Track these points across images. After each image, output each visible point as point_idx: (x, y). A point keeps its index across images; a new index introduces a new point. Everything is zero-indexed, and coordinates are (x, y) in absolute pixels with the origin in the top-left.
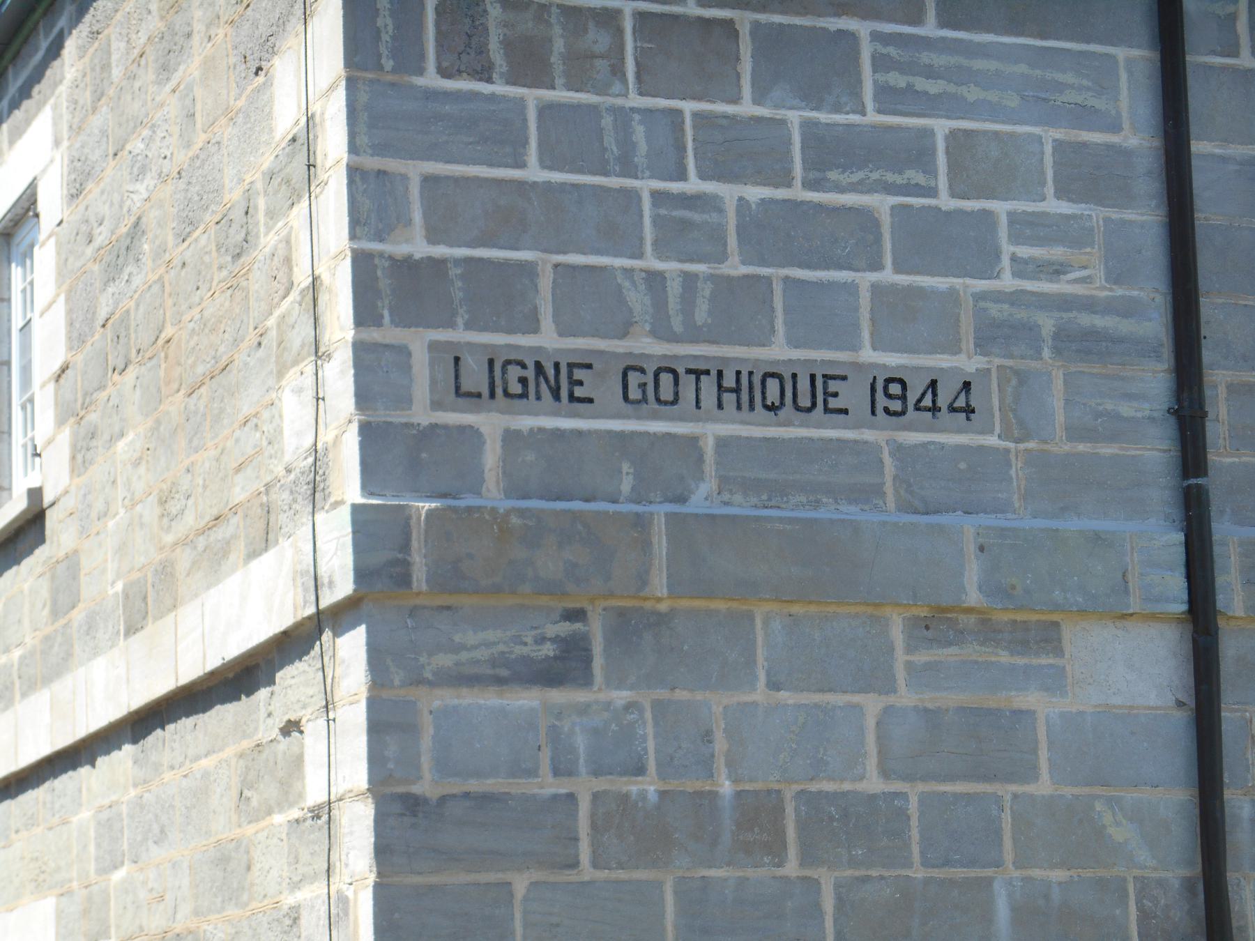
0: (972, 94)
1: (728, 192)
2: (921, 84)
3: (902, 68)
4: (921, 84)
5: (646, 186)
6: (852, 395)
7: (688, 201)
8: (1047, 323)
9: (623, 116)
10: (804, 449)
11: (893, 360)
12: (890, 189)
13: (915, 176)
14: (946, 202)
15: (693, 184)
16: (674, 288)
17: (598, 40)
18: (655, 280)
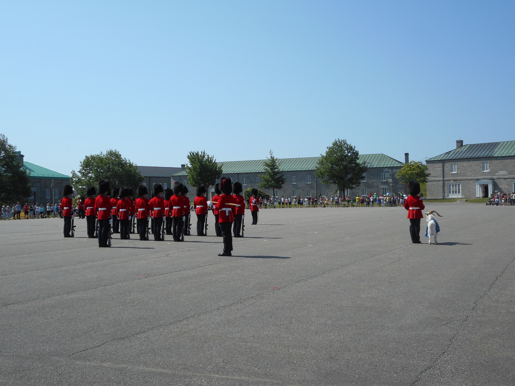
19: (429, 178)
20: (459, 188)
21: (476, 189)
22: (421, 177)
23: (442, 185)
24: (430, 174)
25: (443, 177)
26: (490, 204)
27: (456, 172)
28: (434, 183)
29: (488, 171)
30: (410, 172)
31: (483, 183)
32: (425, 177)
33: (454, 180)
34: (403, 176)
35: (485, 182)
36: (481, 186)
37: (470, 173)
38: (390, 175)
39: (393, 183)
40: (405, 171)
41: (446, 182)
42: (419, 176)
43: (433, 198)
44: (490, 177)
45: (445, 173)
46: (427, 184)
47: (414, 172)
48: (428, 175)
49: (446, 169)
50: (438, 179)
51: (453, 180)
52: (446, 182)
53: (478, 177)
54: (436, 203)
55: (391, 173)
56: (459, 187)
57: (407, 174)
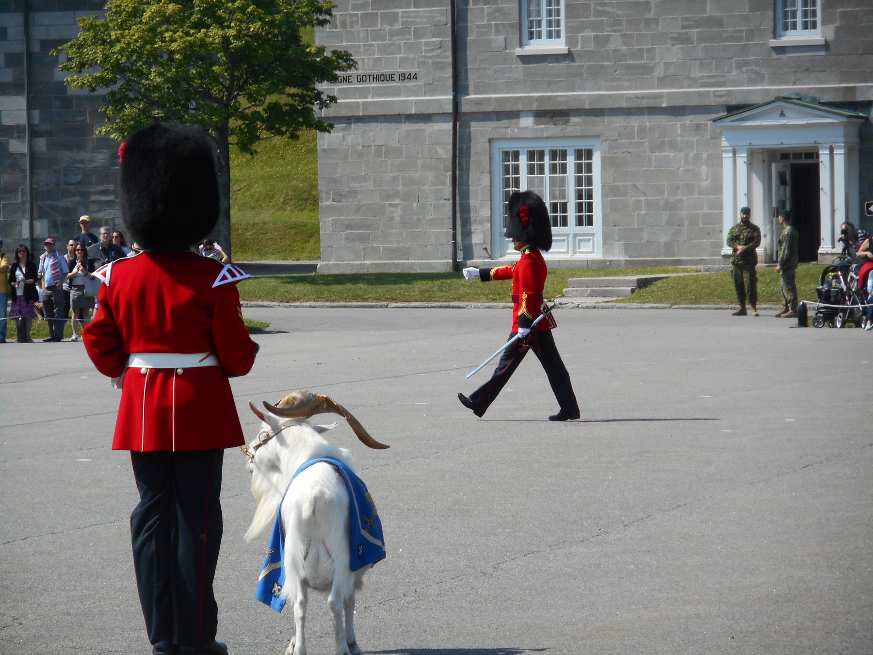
0: (418, 20)
1: (376, 43)
2: (409, 19)
3: (407, 17)
4: (409, 19)
5: (362, 44)
6: (396, 77)
7: (370, 45)
8: (430, 61)
9: (358, 32)
10: (387, 87)
11: (402, 70)
12: (403, 39)
13: (408, 37)
14: (413, 41)
15: (370, 42)
16: (366, 61)
17: (355, 19)
18: (362, 59)
19: (344, 95)
20: (584, 181)
21: (717, 189)
22: (275, 88)
23: (446, 152)
24: (344, 59)
25: (459, 87)
26: (828, 318)
27: (559, 46)
28: (379, 133)
29: (815, 36)
30: (176, 41)
31: (774, 141)
32: (305, 83)
33: (551, 114)
34: (118, 68)
35: (791, 129)
36: (766, 158)
37: (674, 53)
38: (11, 60)
39: (34, 133)
40: (135, 32)
41: (475, 127)
42: (255, 75)
43: (368, 264)
44: (829, 86)
45: (471, 54)
46: (324, 140)
47: (215, 34)
48: (331, 66)
49: (478, 17)
50: (410, 99)
51: (540, 115)
52: (475, 127)
53: (741, 89)
54: (393, 312)
55: (15, 44)
56: (584, 167)
57: (154, 58)
